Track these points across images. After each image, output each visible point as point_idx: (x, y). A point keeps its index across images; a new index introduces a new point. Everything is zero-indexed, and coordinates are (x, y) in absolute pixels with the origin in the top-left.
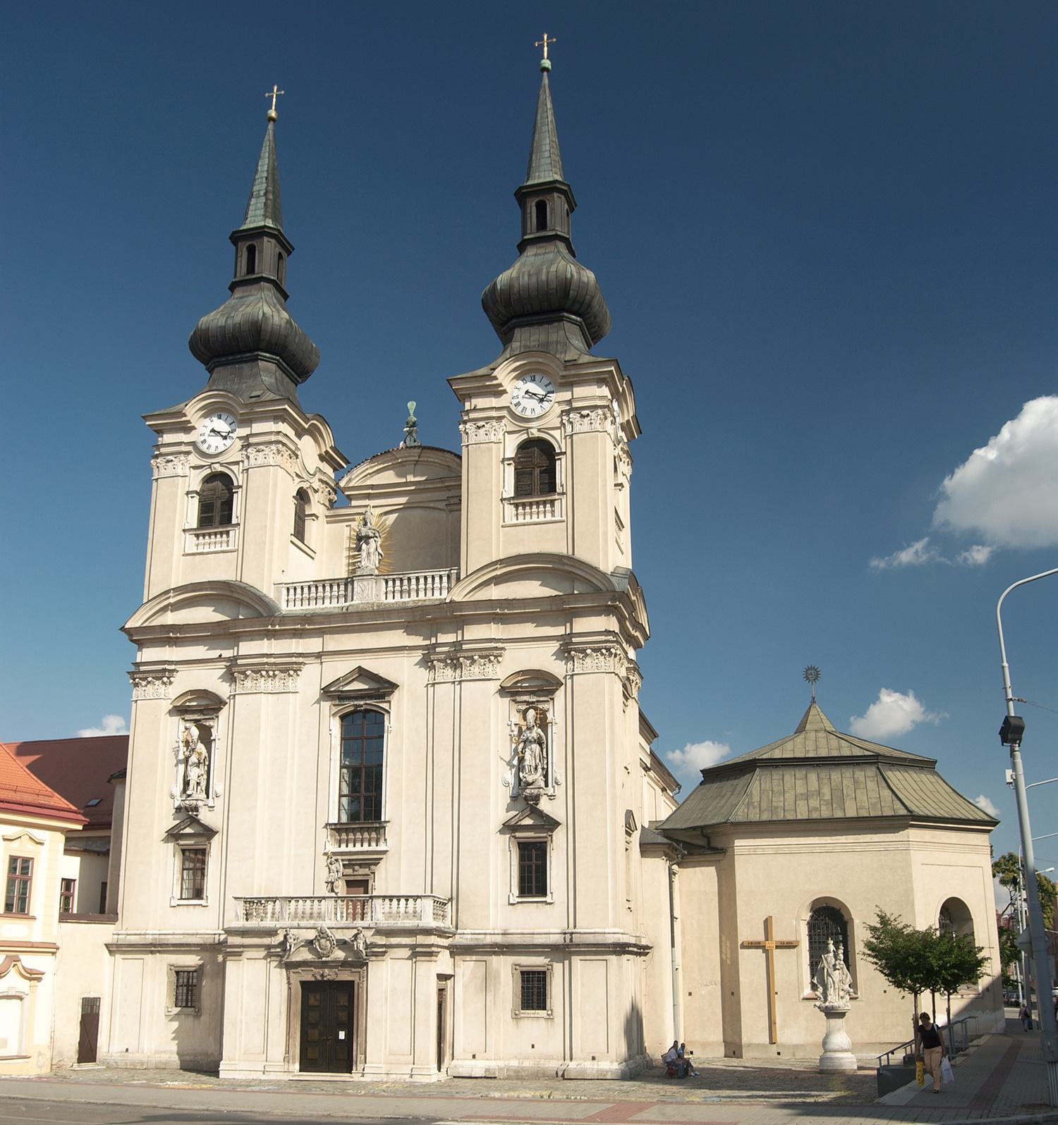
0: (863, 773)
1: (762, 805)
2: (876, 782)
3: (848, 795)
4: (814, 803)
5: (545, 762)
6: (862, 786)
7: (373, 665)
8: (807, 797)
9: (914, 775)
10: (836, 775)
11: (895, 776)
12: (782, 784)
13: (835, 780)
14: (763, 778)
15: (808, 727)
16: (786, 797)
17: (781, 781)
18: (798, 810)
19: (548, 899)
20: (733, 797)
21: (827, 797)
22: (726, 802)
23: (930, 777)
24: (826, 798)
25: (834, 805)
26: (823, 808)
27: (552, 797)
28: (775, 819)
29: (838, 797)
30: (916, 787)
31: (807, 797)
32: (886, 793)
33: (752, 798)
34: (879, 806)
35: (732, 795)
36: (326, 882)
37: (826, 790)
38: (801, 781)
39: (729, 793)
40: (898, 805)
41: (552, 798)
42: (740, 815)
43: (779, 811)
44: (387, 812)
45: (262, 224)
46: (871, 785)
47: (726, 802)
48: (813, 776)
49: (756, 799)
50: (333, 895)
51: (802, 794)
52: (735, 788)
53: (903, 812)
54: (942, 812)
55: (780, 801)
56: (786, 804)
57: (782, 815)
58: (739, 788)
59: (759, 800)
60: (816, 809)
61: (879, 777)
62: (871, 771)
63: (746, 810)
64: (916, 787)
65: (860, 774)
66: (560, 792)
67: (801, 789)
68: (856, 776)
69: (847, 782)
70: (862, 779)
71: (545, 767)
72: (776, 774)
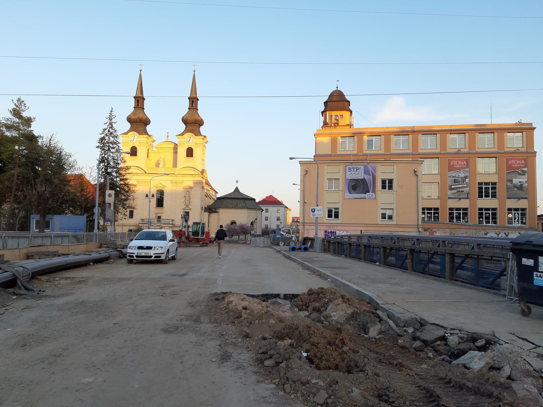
4: (233, 205)
7: (162, 182)
8: (232, 204)
10: (237, 201)
27: (190, 205)
45: (140, 96)
48: (234, 201)
62: (243, 200)
65: (241, 201)
69: (239, 202)
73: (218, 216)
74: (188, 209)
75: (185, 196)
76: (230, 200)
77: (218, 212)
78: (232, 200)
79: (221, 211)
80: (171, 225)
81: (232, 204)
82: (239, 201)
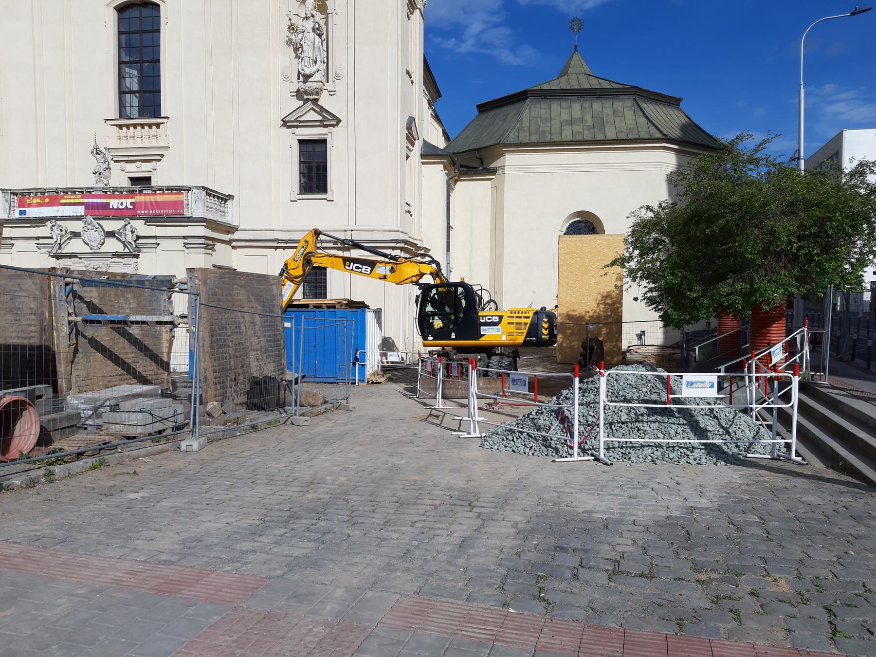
0: (621, 104)
1: (531, 129)
2: (633, 112)
3: (608, 122)
4: (576, 128)
5: (325, 55)
6: (620, 115)
9: (664, 110)
10: (597, 105)
11: (649, 108)
12: (549, 112)
13: (596, 110)
14: (532, 107)
15: (570, 71)
16: (552, 123)
17: (549, 109)
18: (563, 134)
19: (328, 196)
20: (505, 124)
21: (590, 123)
22: (499, 129)
23: (676, 112)
24: (588, 124)
25: (596, 130)
26: (586, 132)
27: (332, 93)
28: (542, 140)
29: (600, 123)
30: (666, 119)
31: (571, 123)
32: (642, 120)
33: (522, 123)
34: (636, 131)
35: (503, 123)
36: (94, 173)
37: (589, 118)
38: (565, 110)
39: (501, 122)
40: (653, 130)
41: (332, 93)
42: (512, 137)
43: (547, 134)
44: (166, 108)
46: (629, 114)
47: (499, 129)
48: (576, 107)
49: (526, 124)
50: (101, 185)
51: (567, 121)
52: (506, 119)
53: (658, 135)
54: (689, 139)
55: (548, 127)
56: (552, 128)
57: (549, 137)
58: (510, 117)
59: (528, 125)
60: (579, 133)
61: (636, 107)
62: (629, 102)
63: (517, 134)
64: (666, 119)
65: (618, 104)
66: (339, 86)
67: (564, 118)
68: (615, 106)
69: (609, 111)
70: (620, 108)
71: (325, 60)
72: (544, 105)
73: (497, 191)
74: (322, 124)
75: (292, 28)
76: (555, 106)
77: (494, 171)
78: (565, 104)
79: (511, 160)
80: (201, 230)
81: (571, 123)
82: (608, 104)
